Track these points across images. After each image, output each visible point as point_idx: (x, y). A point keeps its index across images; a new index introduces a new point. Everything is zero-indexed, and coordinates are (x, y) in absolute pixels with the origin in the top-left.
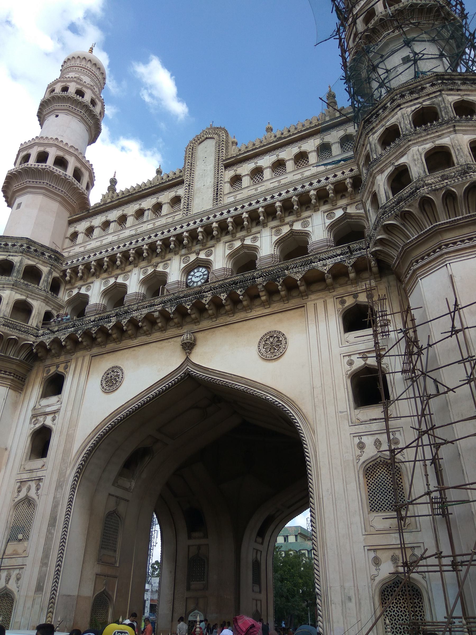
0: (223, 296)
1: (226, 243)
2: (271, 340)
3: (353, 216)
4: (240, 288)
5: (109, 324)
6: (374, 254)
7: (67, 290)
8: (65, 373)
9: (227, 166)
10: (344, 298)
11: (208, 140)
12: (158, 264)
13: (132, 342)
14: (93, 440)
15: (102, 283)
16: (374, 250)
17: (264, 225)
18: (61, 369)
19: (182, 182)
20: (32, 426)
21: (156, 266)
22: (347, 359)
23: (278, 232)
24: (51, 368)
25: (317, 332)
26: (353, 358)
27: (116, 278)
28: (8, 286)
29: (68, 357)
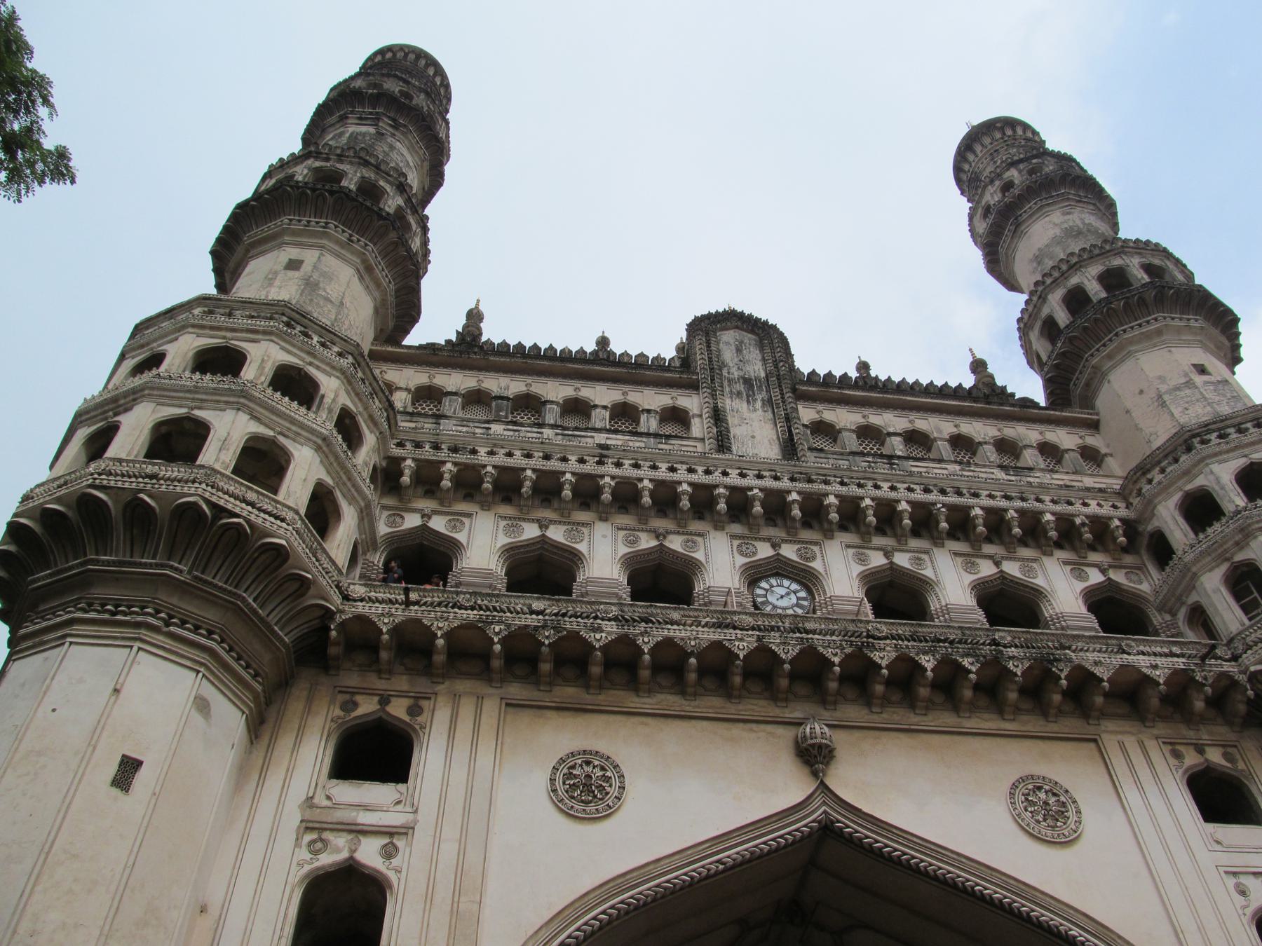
0: (928, 662)
1: (848, 546)
2: (1042, 795)
4: (968, 655)
5: (598, 636)
7: (384, 507)
8: (417, 727)
10: (1178, 747)
13: (637, 700)
17: (937, 541)
19: (694, 386)
20: (304, 854)
21: (665, 537)
23: (970, 567)
24: (359, 698)
25: (1148, 806)
28: (310, 436)
29: (422, 685)
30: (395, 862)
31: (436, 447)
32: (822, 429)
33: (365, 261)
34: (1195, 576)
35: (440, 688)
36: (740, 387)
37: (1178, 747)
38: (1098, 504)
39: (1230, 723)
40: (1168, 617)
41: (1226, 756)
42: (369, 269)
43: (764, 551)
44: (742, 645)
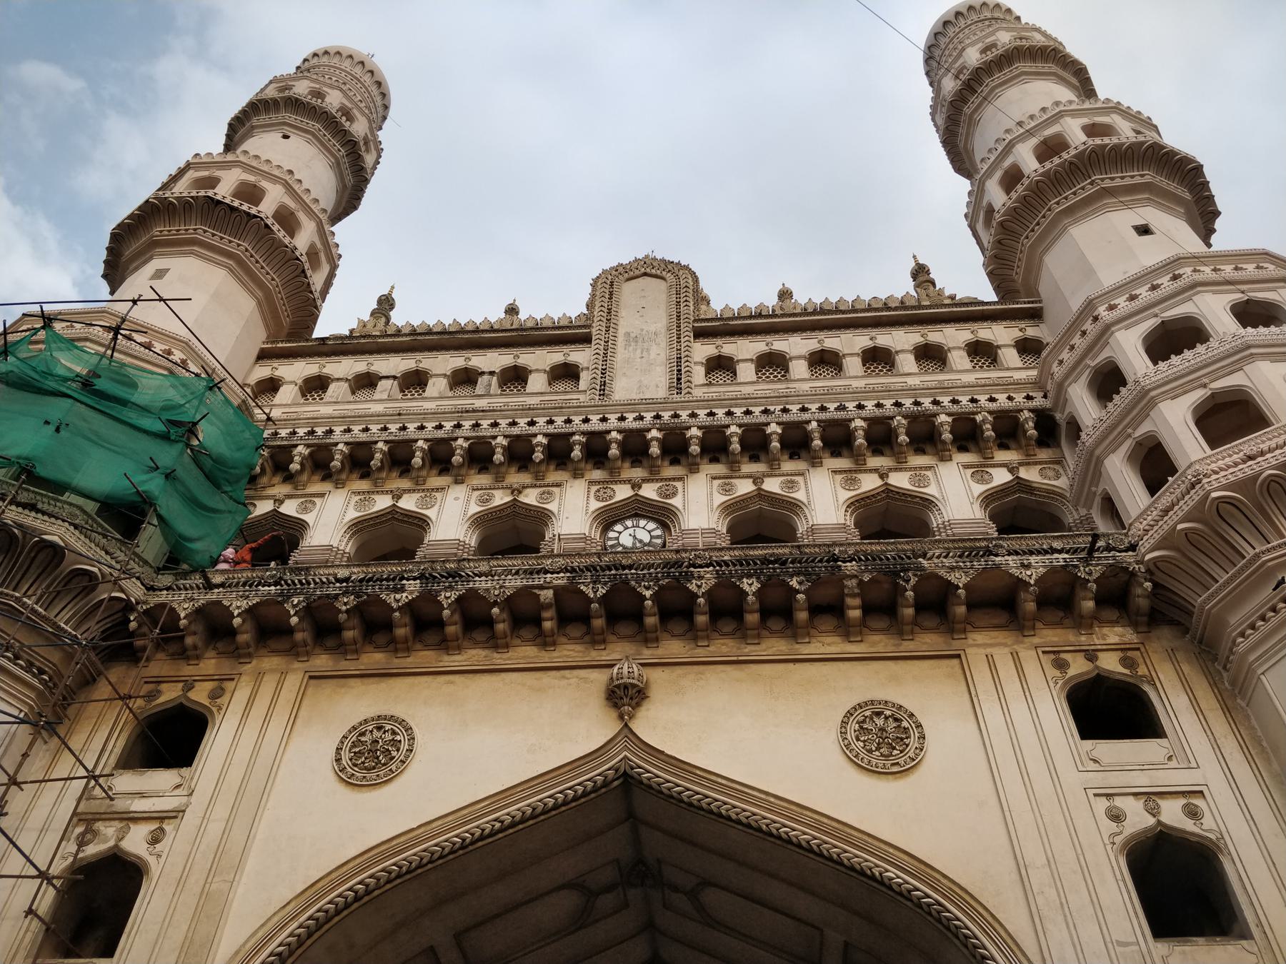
0: (750, 586)
1: (714, 478)
2: (880, 722)
3: (1035, 489)
4: (798, 574)
5: (398, 596)
8: (214, 709)
9: (700, 334)
10: (1063, 656)
11: (649, 279)
12: (524, 487)
14: (296, 924)
15: (353, 503)
17: (815, 462)
18: (200, 695)
19: (586, 340)
21: (520, 492)
23: (851, 482)
24: (163, 687)
26: (1118, 802)
34: (1100, 462)
37: (1063, 656)
38: (1010, 398)
39: (1134, 625)
40: (1083, 512)
41: (1125, 662)
43: (623, 492)
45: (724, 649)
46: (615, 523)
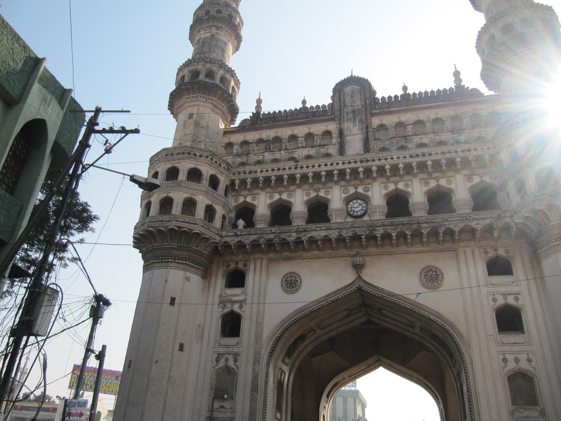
2: (431, 273)
4: (408, 228)
6: (516, 223)
7: (233, 196)
12: (319, 189)
16: (517, 221)
17: (415, 175)
18: (241, 266)
19: (333, 120)
20: (221, 309)
21: (319, 191)
22: (492, 297)
23: (427, 183)
24: (230, 263)
27: (281, 194)
30: (242, 309)
31: (245, 173)
32: (382, 127)
33: (213, 104)
35: (252, 257)
36: (351, 116)
37: (488, 250)
38: (482, 149)
42: (215, 106)
43: (352, 190)
44: (334, 235)
45: (386, 250)
46: (350, 202)
